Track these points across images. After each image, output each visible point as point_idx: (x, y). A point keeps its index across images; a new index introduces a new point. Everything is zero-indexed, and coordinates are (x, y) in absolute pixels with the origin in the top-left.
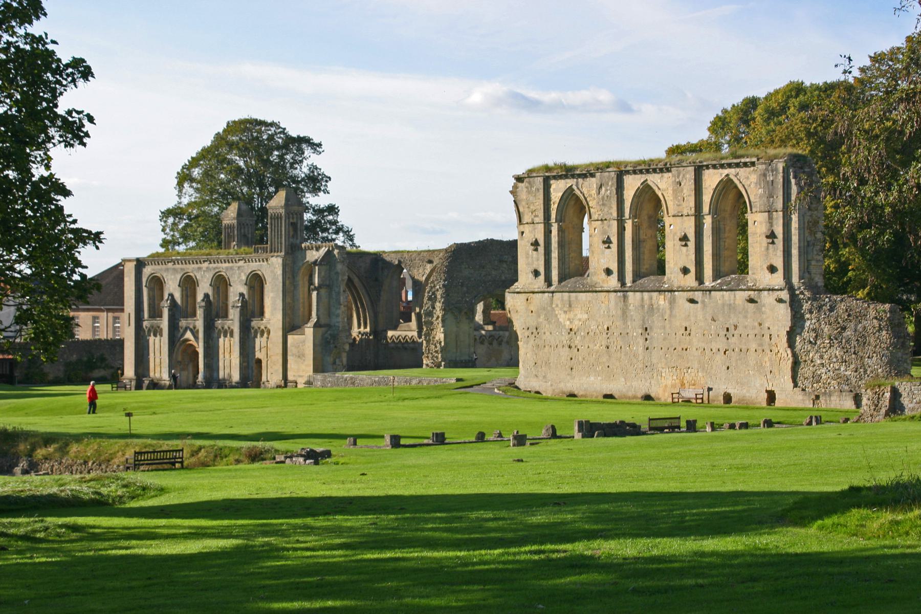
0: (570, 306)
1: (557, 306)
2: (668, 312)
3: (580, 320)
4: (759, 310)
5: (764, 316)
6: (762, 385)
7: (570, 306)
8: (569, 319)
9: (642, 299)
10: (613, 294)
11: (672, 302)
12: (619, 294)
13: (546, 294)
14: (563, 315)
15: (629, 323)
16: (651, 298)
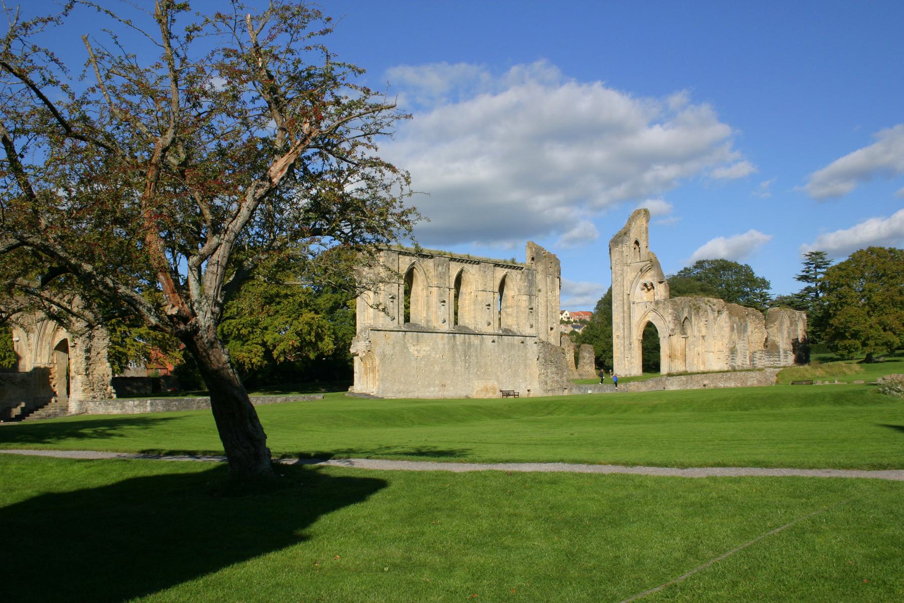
0: (418, 341)
1: (408, 341)
2: (479, 347)
3: (424, 351)
4: (525, 347)
5: (527, 350)
6: (526, 387)
7: (418, 341)
8: (417, 350)
9: (465, 339)
10: (447, 335)
11: (482, 341)
12: (450, 335)
13: (401, 333)
14: (412, 348)
15: (456, 353)
16: (470, 339)
